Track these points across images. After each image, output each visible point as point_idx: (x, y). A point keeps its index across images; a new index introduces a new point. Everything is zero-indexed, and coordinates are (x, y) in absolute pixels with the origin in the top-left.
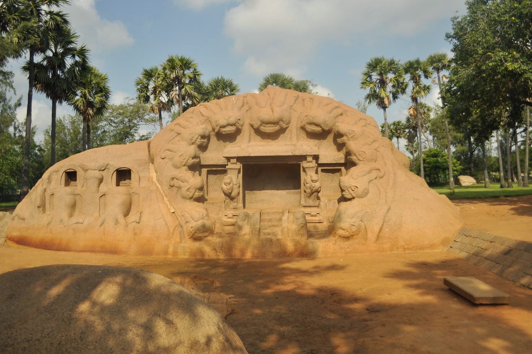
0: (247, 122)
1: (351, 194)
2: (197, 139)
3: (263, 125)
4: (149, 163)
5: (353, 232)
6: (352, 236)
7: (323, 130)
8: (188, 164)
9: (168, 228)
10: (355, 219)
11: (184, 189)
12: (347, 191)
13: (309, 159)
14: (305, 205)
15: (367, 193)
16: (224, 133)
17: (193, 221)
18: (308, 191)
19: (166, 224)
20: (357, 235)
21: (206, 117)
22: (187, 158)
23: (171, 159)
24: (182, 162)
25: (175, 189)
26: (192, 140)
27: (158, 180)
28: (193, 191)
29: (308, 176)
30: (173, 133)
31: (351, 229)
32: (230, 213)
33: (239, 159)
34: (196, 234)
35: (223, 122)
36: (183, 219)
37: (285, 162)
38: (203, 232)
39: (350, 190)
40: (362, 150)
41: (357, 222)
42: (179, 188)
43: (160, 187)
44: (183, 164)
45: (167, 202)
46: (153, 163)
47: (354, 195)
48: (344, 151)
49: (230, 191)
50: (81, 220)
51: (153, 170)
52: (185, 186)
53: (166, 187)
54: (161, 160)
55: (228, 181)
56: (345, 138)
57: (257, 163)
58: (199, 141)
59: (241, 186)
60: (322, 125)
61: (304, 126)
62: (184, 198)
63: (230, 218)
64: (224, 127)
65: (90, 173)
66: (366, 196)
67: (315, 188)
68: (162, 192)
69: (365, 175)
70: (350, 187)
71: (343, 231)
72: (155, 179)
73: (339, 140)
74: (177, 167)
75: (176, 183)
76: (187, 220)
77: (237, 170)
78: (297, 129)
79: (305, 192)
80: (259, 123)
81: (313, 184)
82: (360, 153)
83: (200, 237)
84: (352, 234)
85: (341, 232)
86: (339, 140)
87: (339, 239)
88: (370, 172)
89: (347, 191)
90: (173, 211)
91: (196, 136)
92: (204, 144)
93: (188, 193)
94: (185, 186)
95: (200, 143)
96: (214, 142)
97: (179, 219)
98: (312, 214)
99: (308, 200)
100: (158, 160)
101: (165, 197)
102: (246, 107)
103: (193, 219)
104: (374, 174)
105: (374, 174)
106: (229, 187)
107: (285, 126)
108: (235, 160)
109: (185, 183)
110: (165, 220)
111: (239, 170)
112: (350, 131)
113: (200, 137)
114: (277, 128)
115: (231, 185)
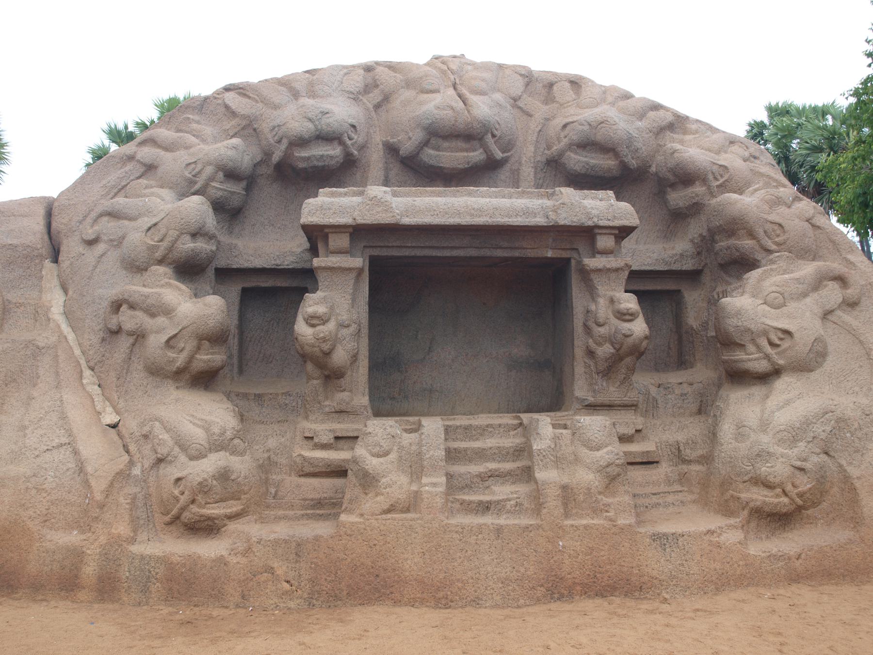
0: (378, 138)
1: (767, 357)
2: (211, 179)
3: (433, 141)
4: (41, 257)
5: (801, 495)
6: (800, 509)
7: (624, 166)
8: (175, 255)
9: (87, 484)
10: (802, 445)
11: (155, 342)
12: (751, 348)
13: (605, 242)
14: (591, 399)
15: (822, 355)
16: (301, 165)
17: (183, 458)
18: (606, 350)
20: (815, 504)
21: (244, 117)
22: (173, 234)
23: (118, 242)
24: (152, 249)
25: (125, 343)
26: (191, 182)
27: (67, 314)
28: (189, 346)
29: (601, 301)
30: (129, 167)
31: (794, 486)
32: (324, 429)
33: (361, 233)
34: (194, 508)
35: (299, 126)
36: (147, 449)
37: (517, 254)
38: (222, 500)
39: (764, 343)
40: (773, 217)
41: (815, 459)
42: (139, 336)
43: (71, 337)
44: (158, 254)
45: (95, 390)
46: (56, 260)
47: (781, 362)
48: (696, 228)
49: (326, 347)
51: (55, 282)
52: (159, 332)
53: (93, 338)
54: (81, 249)
55: (321, 309)
56: (698, 189)
57: (419, 253)
58: (220, 187)
59: (365, 331)
60: (624, 151)
61: (561, 154)
62: (156, 371)
63: (324, 447)
64: (301, 142)
66: (820, 365)
67: (630, 341)
68: (77, 352)
69: (805, 295)
70: (765, 333)
71: (766, 492)
72: (56, 312)
73: (678, 198)
74: (136, 267)
75: (128, 319)
76: (163, 451)
77: (353, 275)
78: (536, 168)
79: (591, 353)
80: (418, 136)
81: (625, 326)
82: (768, 227)
83: (209, 518)
84: (799, 502)
85: (759, 496)
86: (678, 198)
87: (753, 524)
88: (817, 284)
89: (751, 348)
90: (110, 417)
91: (209, 170)
92: (236, 202)
93: (171, 354)
94: (159, 332)
95: (220, 193)
96: (268, 193)
97: (132, 448)
99: (601, 383)
100: (71, 247)
101: (87, 373)
102: (376, 96)
103: (184, 448)
106: (325, 330)
107: (499, 155)
108: (341, 241)
109: (161, 320)
110: (76, 452)
111: (360, 271)
112: (715, 168)
113: (221, 175)
114: (477, 156)
115: (331, 326)
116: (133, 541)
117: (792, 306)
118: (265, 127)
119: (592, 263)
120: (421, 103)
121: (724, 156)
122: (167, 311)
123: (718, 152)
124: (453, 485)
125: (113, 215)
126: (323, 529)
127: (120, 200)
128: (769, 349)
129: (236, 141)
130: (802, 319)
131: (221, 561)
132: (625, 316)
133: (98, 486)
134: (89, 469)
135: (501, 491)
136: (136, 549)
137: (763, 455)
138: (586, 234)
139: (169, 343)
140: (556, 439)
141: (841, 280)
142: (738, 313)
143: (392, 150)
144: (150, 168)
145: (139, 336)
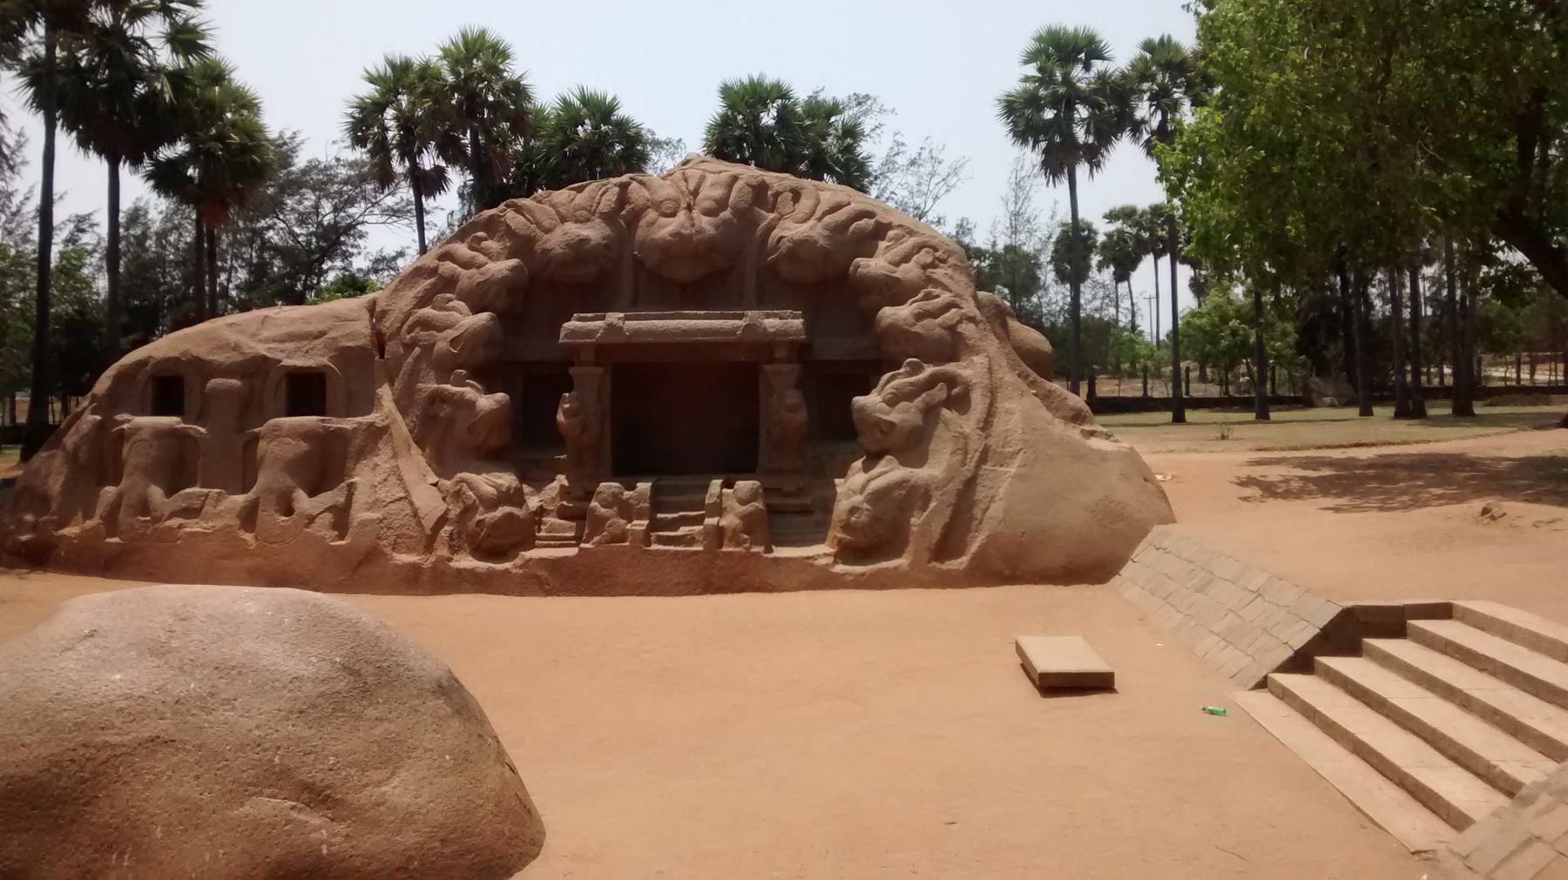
9: (419, 524)
19: (415, 514)
42: (450, 421)
50: (197, 504)
65: (215, 382)
88: (931, 383)
98: (786, 488)
104: (940, 392)
105: (940, 392)
110: (411, 503)
116: (450, 560)
117: (903, 405)
118: (538, 247)
119: (768, 368)
120: (662, 227)
121: (903, 266)
122: (471, 404)
123: (897, 264)
124: (655, 525)
125: (426, 324)
126: (571, 552)
127: (428, 311)
128: (879, 436)
129: (513, 262)
130: (904, 415)
131: (507, 571)
132: (793, 409)
133: (428, 524)
134: (421, 514)
135: (683, 530)
136: (452, 564)
137: (853, 510)
138: (764, 347)
139: (470, 429)
140: (720, 496)
141: (951, 381)
142: (862, 409)
143: (638, 263)
144: (449, 283)
145: (450, 421)
